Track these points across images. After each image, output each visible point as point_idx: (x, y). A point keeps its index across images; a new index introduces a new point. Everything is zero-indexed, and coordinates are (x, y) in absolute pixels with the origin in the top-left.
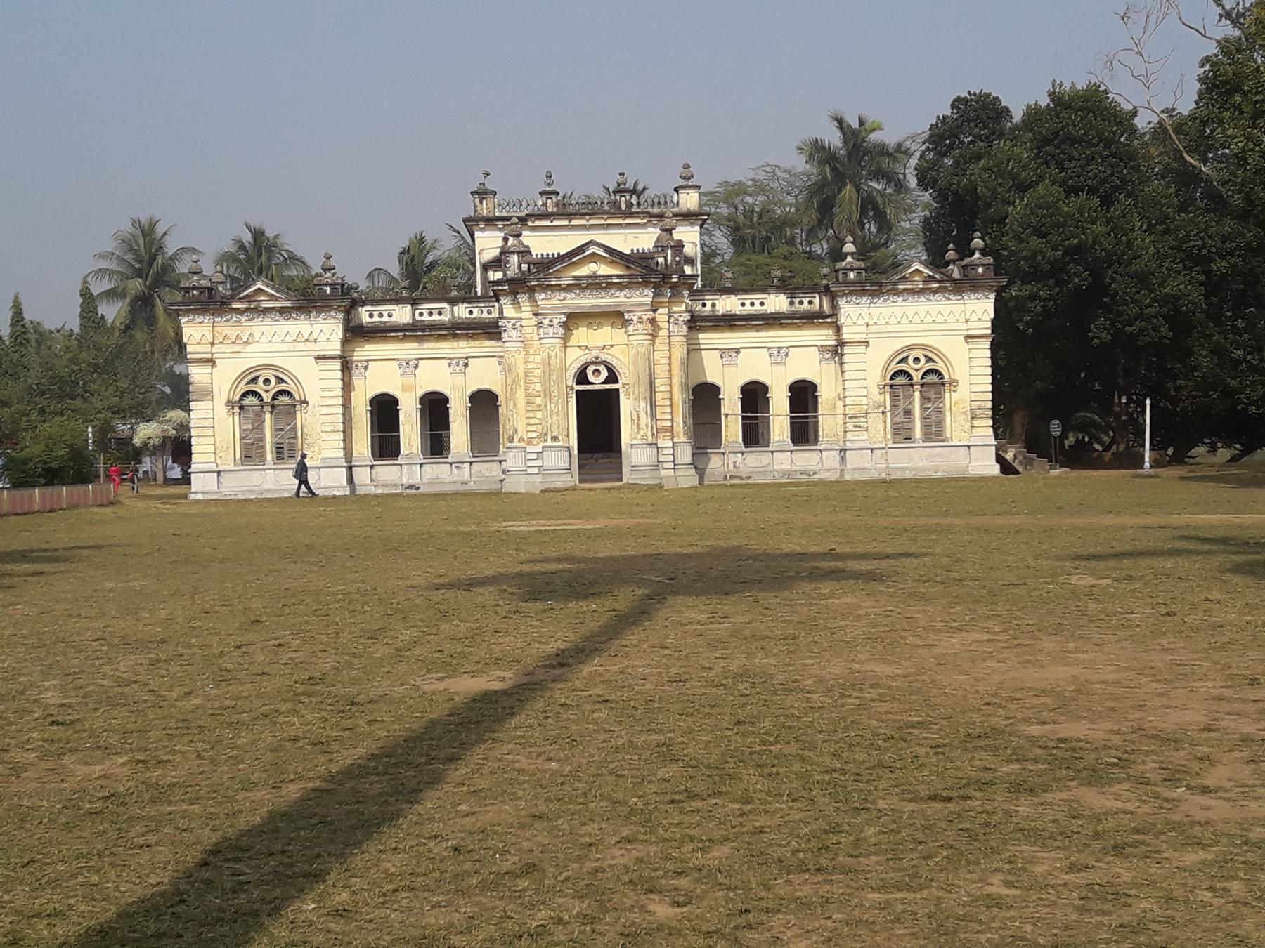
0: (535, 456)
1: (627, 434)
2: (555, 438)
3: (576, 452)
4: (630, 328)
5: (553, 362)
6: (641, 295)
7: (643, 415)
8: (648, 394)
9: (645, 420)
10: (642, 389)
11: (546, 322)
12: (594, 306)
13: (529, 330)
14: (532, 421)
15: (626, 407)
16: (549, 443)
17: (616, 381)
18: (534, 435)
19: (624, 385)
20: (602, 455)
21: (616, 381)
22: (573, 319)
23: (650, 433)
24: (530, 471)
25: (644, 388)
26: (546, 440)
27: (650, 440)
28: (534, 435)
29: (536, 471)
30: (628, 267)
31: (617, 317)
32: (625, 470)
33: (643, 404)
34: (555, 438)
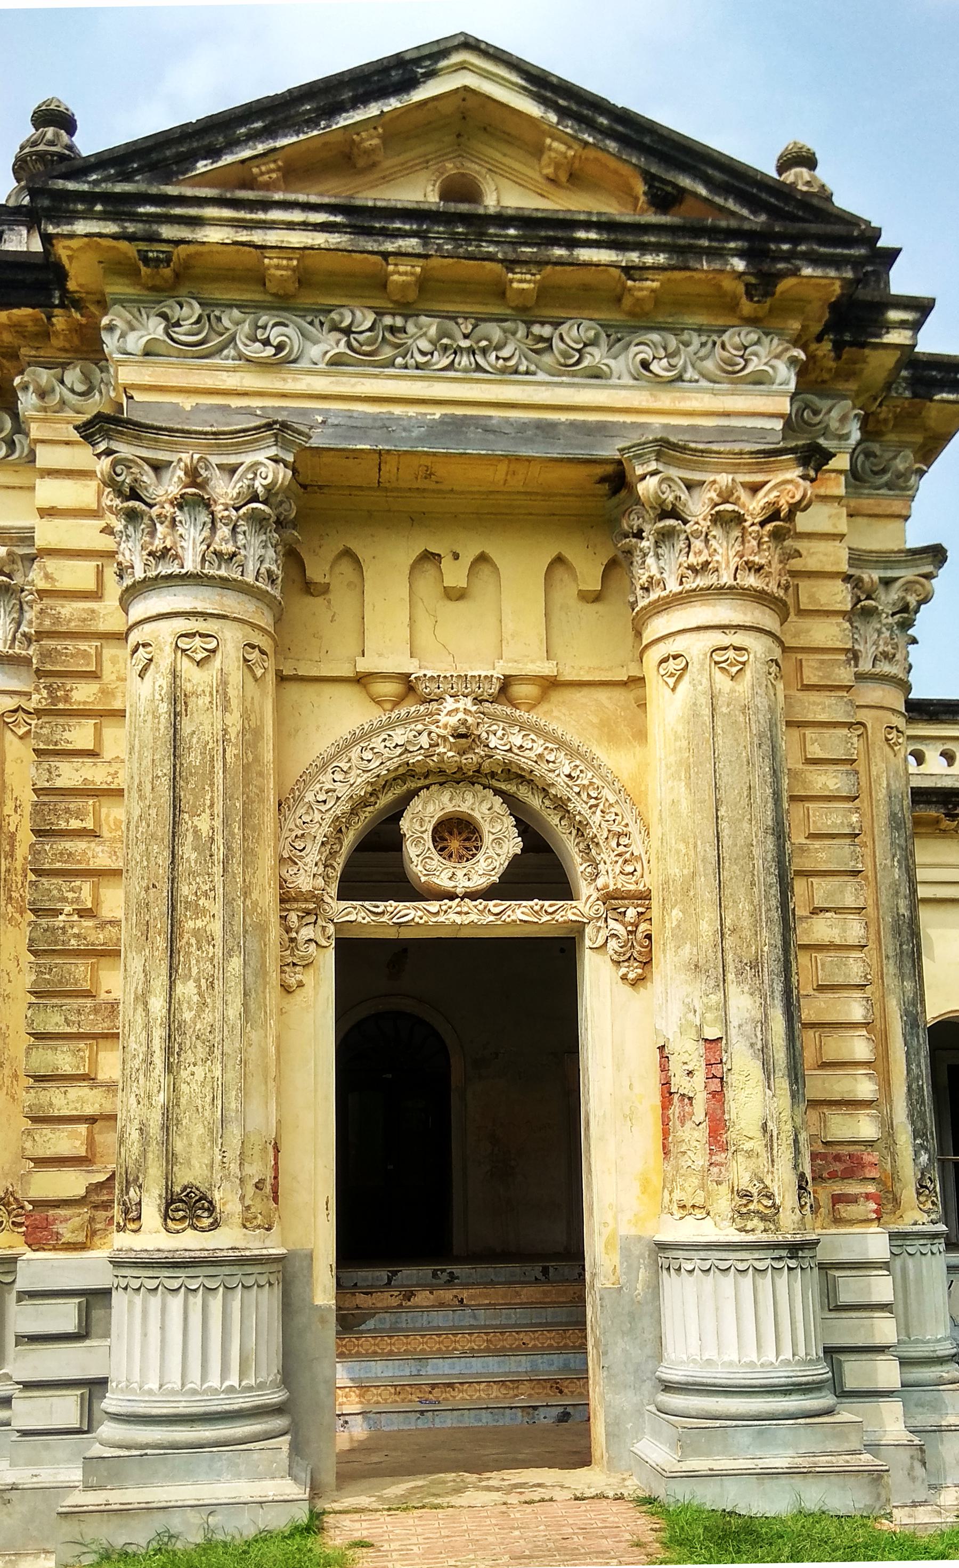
0: (64, 1316)
1: (625, 1185)
2: (188, 1206)
3: (323, 1291)
4: (661, 568)
5: (202, 724)
6: (734, 375)
7: (743, 1064)
8: (768, 940)
9: (754, 1100)
10: (740, 911)
11: (171, 486)
12: (455, 427)
13: (79, 575)
14: (63, 1100)
15: (625, 1034)
16: (153, 1236)
17: (558, 886)
18: (72, 1183)
19: (613, 899)
20: (426, 1271)
21: (558, 886)
22: (327, 511)
23: (782, 1183)
24: (29, 1412)
25: (749, 905)
26: (132, 1216)
27: (789, 1225)
28: (72, 1183)
29: (65, 1409)
30: (664, 198)
31: (597, 507)
32: (606, 1399)
33: (742, 1003)
34: (188, 1206)
